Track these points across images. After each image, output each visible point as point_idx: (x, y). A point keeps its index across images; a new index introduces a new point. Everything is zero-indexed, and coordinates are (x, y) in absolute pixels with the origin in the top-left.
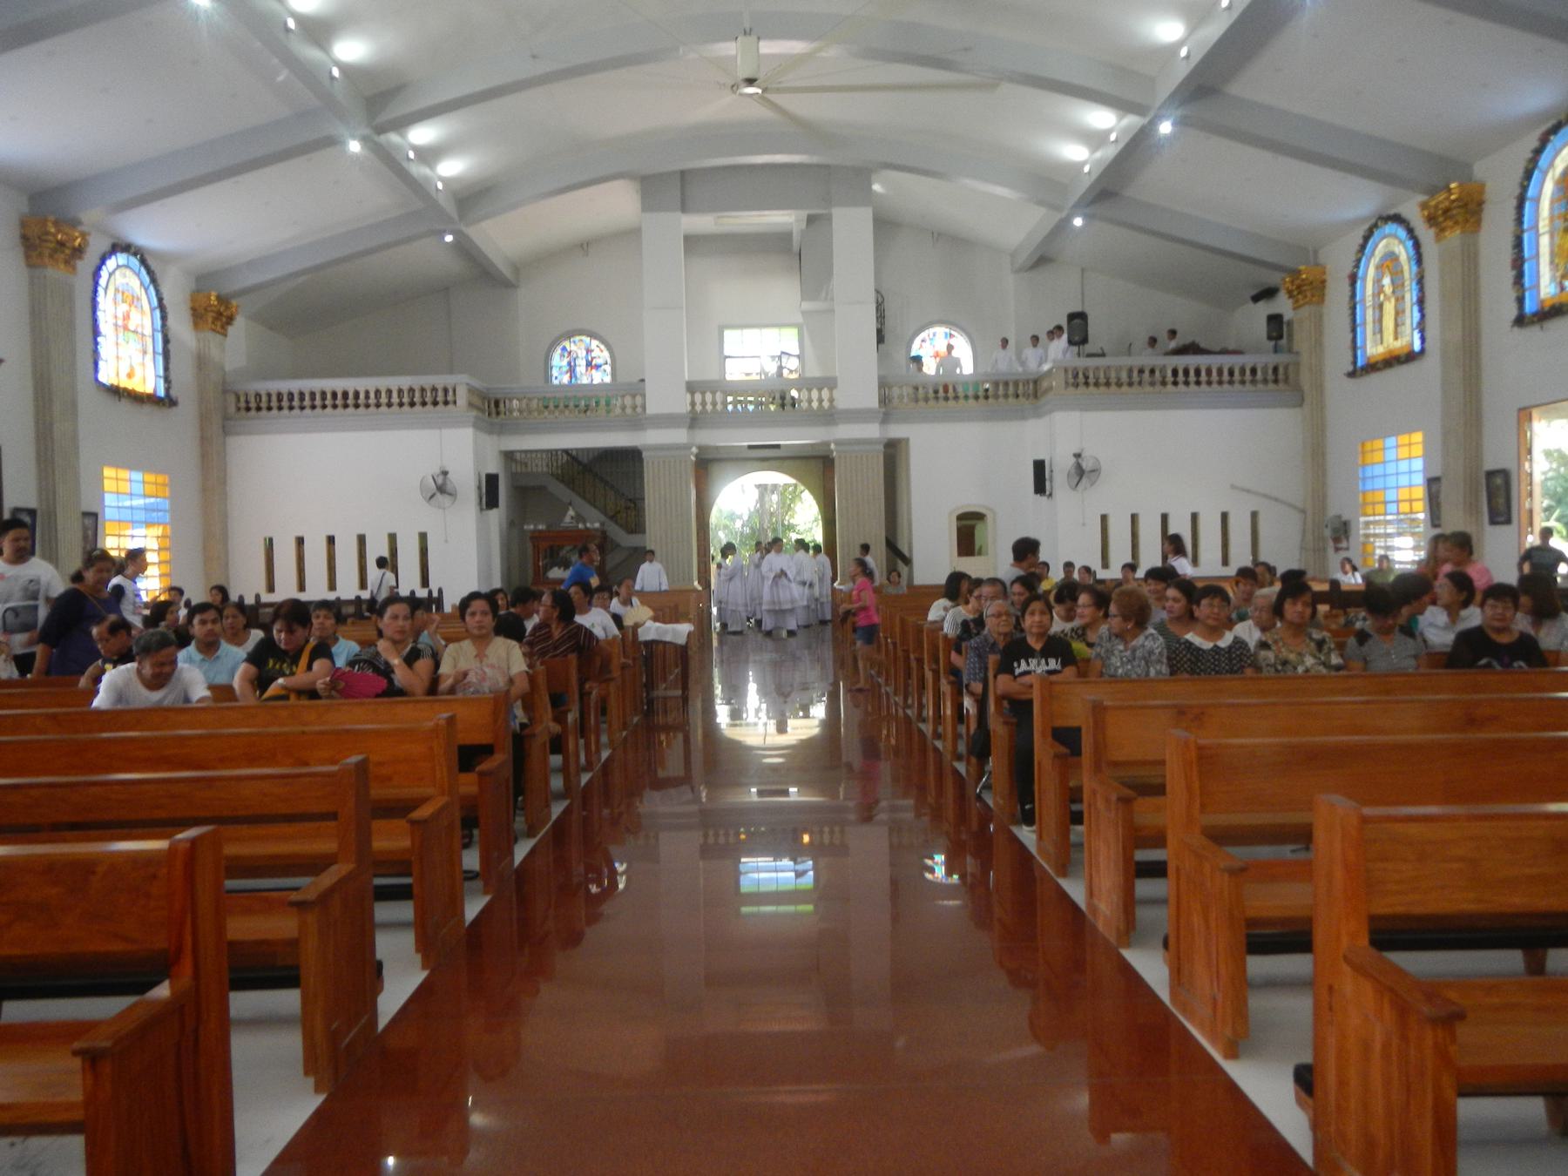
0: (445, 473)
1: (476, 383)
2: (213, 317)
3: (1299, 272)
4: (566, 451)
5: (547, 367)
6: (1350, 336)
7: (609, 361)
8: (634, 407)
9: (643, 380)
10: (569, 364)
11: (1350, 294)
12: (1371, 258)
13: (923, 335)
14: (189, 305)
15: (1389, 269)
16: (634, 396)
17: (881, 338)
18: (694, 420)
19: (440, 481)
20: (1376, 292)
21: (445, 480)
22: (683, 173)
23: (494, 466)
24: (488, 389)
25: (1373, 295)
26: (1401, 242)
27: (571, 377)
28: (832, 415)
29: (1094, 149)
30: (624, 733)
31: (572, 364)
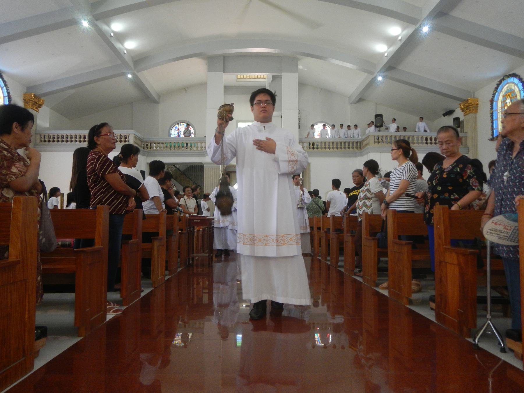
1: (138, 135)
2: (32, 103)
3: (468, 100)
4: (174, 164)
5: (169, 134)
6: (491, 124)
8: (202, 148)
11: (491, 107)
12: (500, 92)
14: (23, 98)
15: (510, 97)
16: (202, 143)
17: (299, 127)
20: (503, 106)
22: (225, 58)
24: (144, 138)
25: (502, 108)
26: (517, 85)
29: (389, 47)
31: (179, 133)
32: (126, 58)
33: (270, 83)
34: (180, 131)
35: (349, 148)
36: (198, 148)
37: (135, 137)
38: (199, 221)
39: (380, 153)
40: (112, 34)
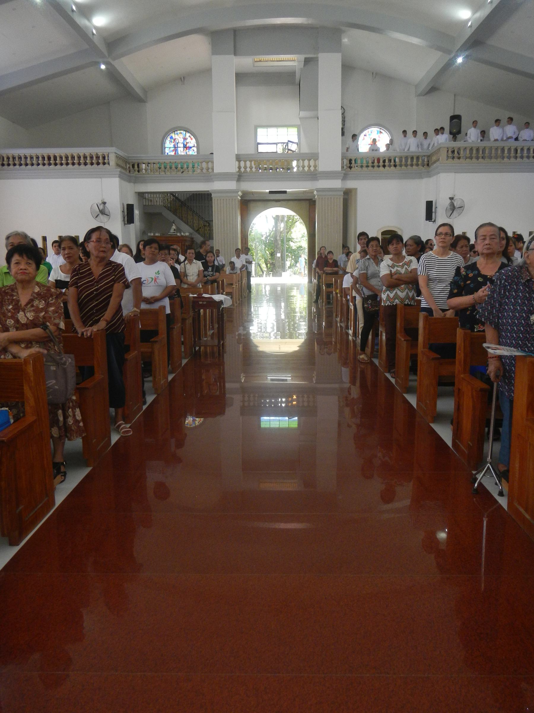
0: (104, 203)
1: (121, 153)
4: (172, 193)
5: (163, 147)
7: (196, 145)
8: (208, 169)
9: (212, 153)
10: (175, 145)
13: (365, 132)
16: (208, 163)
18: (240, 177)
19: (101, 207)
21: (104, 207)
22: (235, 32)
23: (132, 200)
24: (128, 157)
27: (175, 153)
28: (316, 175)
30: (170, 378)
31: (176, 146)
32: (96, 40)
33: (301, 69)
34: (178, 143)
35: (412, 165)
36: (203, 171)
37: (117, 157)
38: (205, 303)
39: (454, 174)
40: (74, 8)
